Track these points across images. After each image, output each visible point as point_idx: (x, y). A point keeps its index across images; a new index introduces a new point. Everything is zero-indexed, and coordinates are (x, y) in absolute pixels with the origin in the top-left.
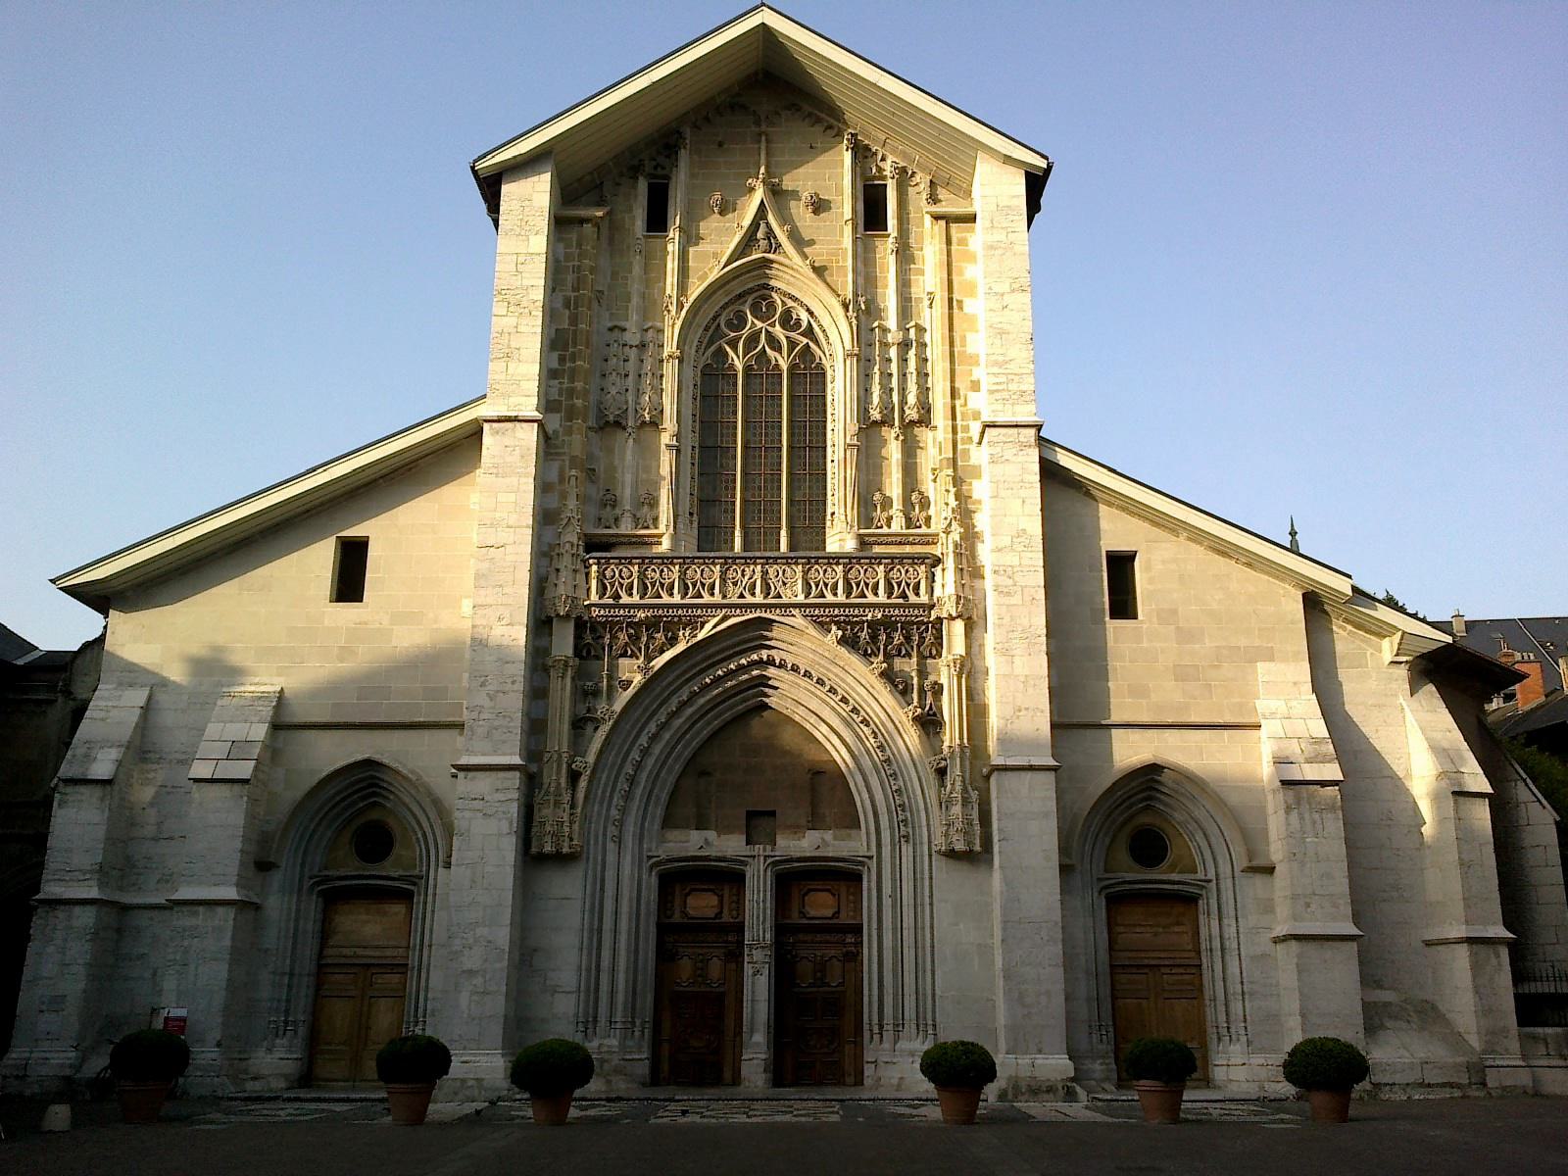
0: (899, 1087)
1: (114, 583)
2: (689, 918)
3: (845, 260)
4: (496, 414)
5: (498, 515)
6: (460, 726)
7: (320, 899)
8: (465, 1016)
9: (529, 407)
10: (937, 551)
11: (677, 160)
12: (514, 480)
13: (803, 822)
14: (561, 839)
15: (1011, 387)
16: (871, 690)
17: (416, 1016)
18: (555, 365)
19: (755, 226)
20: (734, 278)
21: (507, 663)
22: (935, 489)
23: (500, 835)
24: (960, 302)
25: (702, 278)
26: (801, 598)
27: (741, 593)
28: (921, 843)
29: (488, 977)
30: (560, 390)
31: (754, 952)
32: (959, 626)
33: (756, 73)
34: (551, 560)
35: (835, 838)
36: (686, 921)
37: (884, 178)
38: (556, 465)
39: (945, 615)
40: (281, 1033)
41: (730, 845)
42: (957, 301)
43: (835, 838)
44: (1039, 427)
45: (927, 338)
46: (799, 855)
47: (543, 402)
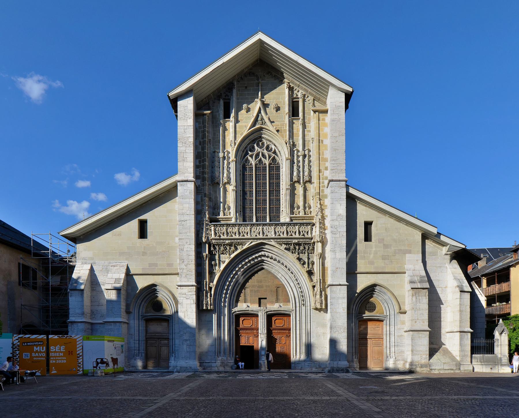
1: (76, 233)
3: (286, 127)
4: (181, 179)
5: (184, 211)
6: (178, 274)
7: (145, 321)
8: (186, 351)
9: (191, 176)
10: (314, 221)
11: (232, 93)
12: (188, 200)
13: (274, 301)
16: (294, 263)
17: (173, 351)
18: (198, 164)
19: (257, 116)
21: (190, 255)
22: (313, 202)
23: (191, 304)
25: (241, 134)
26: (273, 236)
27: (256, 235)
28: (308, 306)
29: (191, 341)
30: (200, 172)
32: (320, 244)
34: (200, 225)
35: (283, 305)
37: (298, 98)
38: (200, 196)
39: (316, 241)
40: (138, 355)
41: (254, 307)
43: (283, 305)
44: (346, 181)
45: (311, 153)
46: (273, 310)
47: (195, 175)
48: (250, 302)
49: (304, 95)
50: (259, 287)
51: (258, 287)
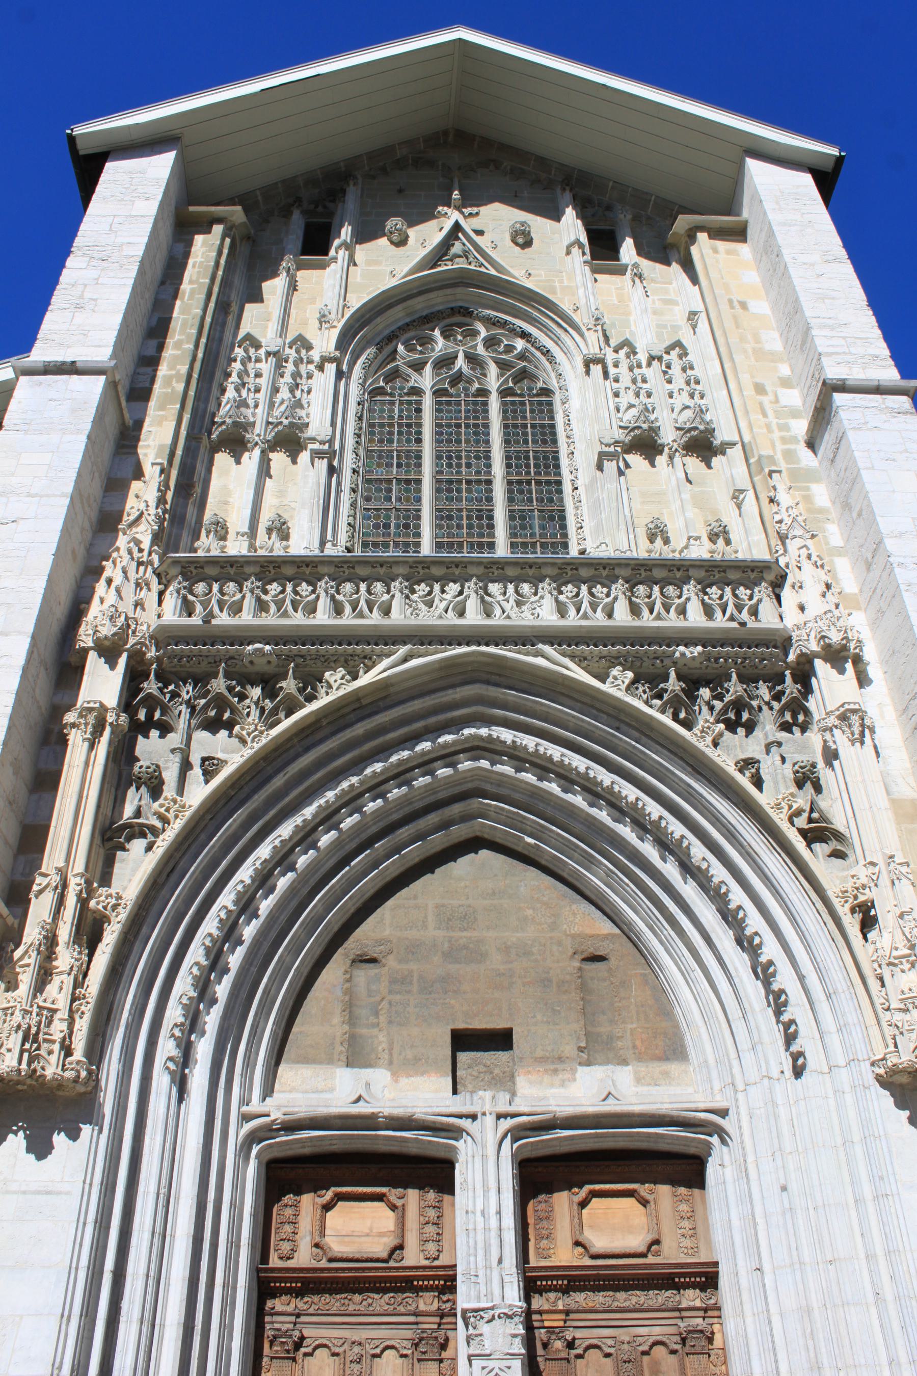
2: (331, 1260)
13: (569, 1049)
14: (45, 1046)
15: (853, 350)
20: (421, 293)
24: (744, 305)
31: (484, 1328)
33: (446, 133)
35: (638, 1080)
36: (324, 1264)
42: (739, 302)
48: (391, 1063)
49: (636, 218)
50: (452, 954)
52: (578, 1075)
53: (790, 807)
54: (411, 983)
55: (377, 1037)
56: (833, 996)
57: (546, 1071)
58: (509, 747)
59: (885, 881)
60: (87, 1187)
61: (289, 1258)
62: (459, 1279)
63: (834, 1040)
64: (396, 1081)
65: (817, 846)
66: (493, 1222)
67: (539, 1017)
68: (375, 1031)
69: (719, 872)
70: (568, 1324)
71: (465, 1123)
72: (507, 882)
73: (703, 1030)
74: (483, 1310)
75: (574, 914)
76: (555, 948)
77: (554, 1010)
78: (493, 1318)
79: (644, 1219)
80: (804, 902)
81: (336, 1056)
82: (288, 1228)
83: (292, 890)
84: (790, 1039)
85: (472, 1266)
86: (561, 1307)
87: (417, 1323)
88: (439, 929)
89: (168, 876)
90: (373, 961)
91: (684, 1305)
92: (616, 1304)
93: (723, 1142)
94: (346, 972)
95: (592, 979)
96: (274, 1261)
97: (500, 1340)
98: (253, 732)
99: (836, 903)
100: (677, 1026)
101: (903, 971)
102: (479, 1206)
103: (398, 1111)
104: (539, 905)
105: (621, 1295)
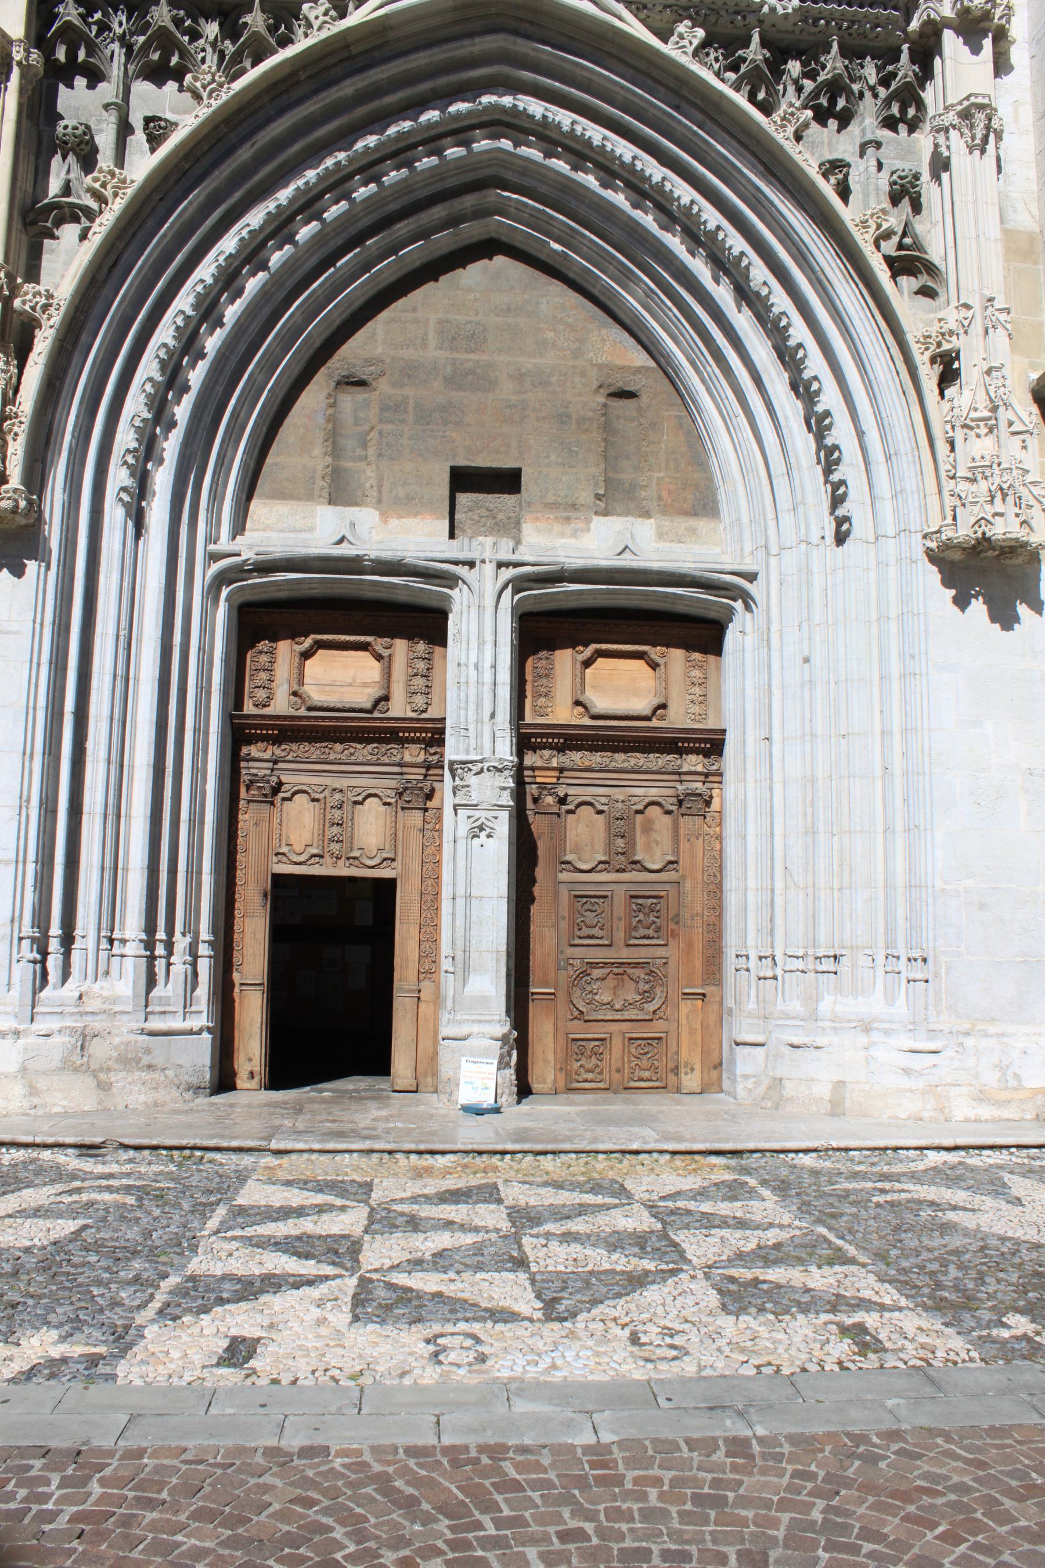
0: (836, 1108)
13: (585, 496)
31: (472, 780)
35: (661, 536)
36: (303, 712)
48: (379, 501)
51: (453, 381)
52: (592, 525)
53: (879, 226)
54: (406, 411)
55: (364, 471)
56: (893, 458)
57: (557, 518)
58: (538, 123)
59: (977, 328)
60: (38, 626)
61: (264, 706)
62: (448, 732)
63: (886, 508)
64: (385, 522)
65: (904, 280)
66: (488, 677)
67: (553, 457)
68: (362, 465)
69: (781, 301)
70: (562, 780)
71: (461, 571)
72: (526, 296)
73: (740, 485)
74: (471, 762)
75: (603, 340)
76: (577, 380)
77: (571, 451)
78: (481, 771)
79: (652, 683)
80: (877, 346)
81: (317, 492)
82: (263, 676)
83: (264, 294)
84: (837, 501)
85: (462, 719)
86: (555, 765)
87: (401, 774)
88: (441, 348)
89: (110, 271)
90: (362, 383)
91: (685, 769)
92: (613, 764)
93: (748, 608)
94: (329, 396)
95: (618, 417)
96: (249, 708)
97: (488, 792)
98: (210, 84)
99: (915, 349)
100: (710, 479)
101: (978, 436)
102: (473, 658)
103: (386, 555)
104: (561, 327)
105: (620, 757)
